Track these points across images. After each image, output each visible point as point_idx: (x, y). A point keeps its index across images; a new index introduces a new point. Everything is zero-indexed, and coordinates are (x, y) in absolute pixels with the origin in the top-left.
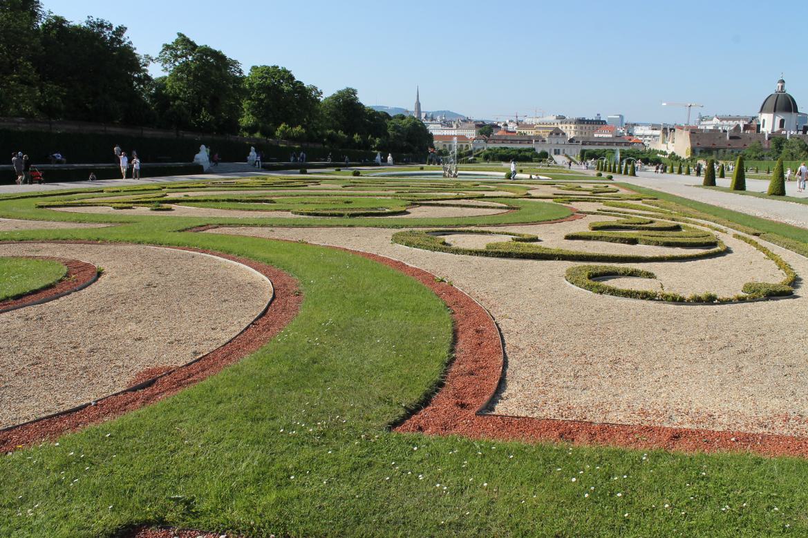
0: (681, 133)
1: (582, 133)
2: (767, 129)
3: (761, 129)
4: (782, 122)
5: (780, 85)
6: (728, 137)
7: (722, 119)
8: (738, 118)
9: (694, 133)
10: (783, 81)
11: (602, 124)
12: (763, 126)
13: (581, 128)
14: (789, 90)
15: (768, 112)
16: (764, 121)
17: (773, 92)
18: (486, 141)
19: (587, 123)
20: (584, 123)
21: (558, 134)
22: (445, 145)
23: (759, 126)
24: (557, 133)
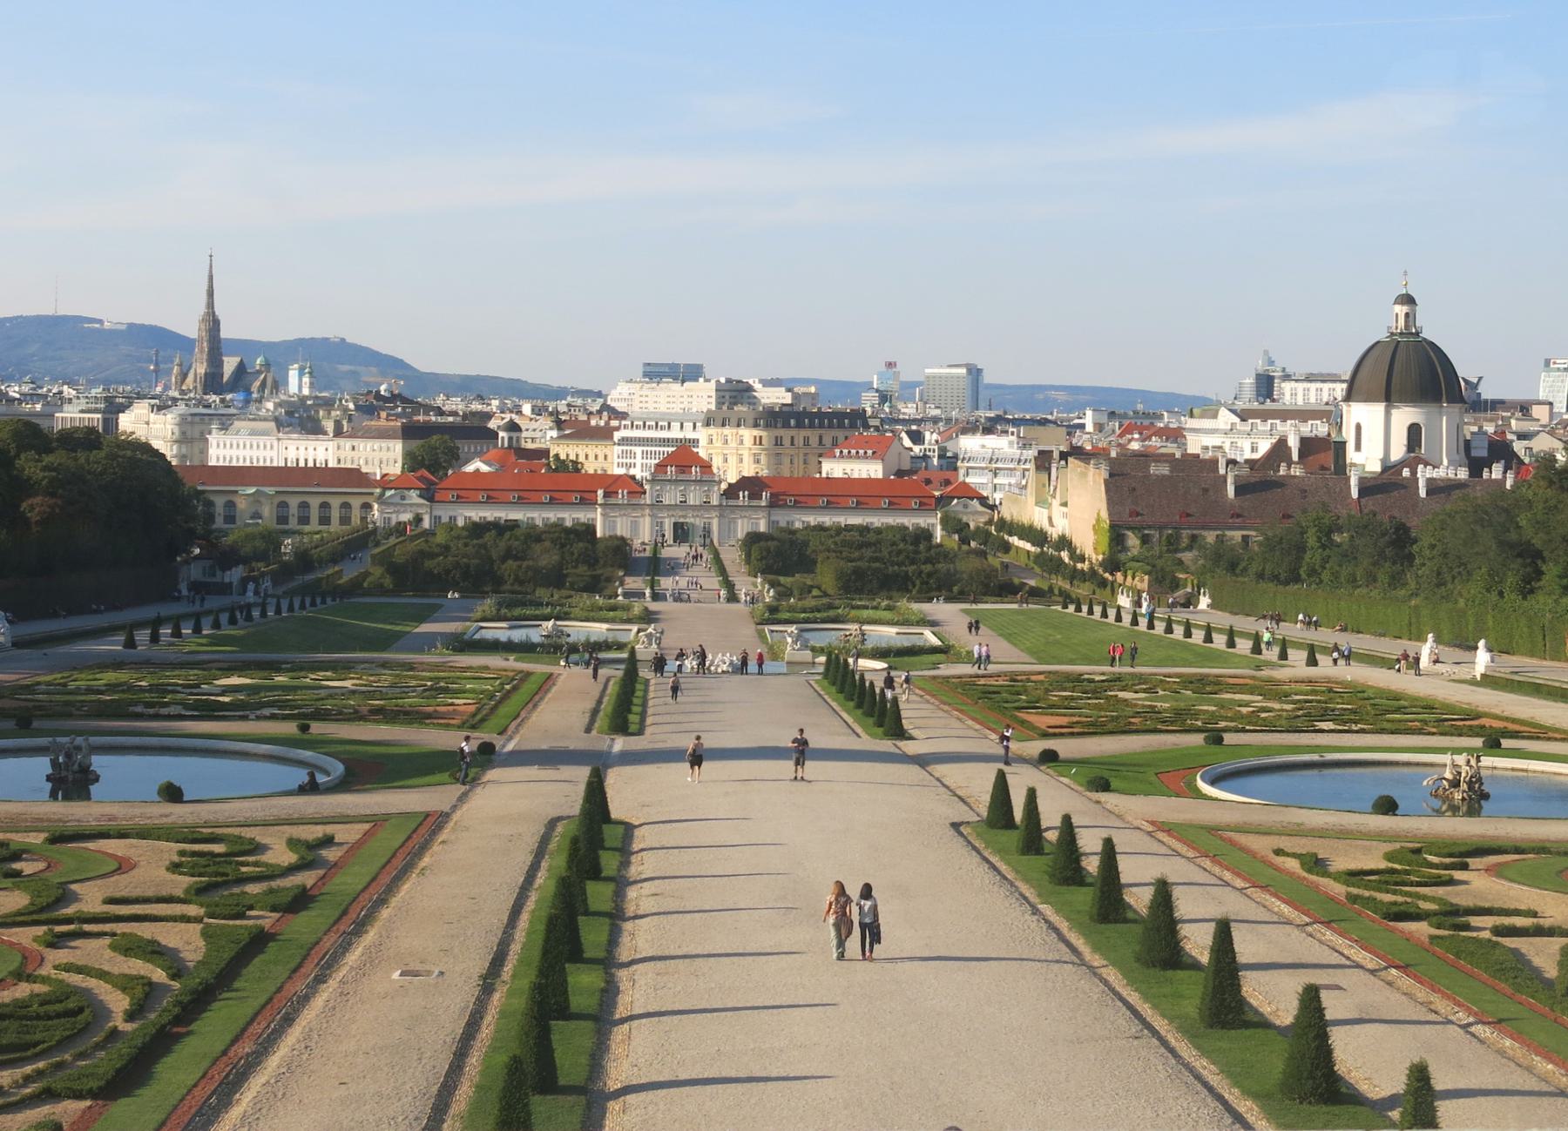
0: (1084, 475)
2: (1366, 459)
3: (1352, 456)
4: (1414, 432)
6: (1231, 490)
10: (1408, 300)
11: (853, 426)
12: (1358, 447)
15: (1369, 398)
16: (1358, 427)
19: (799, 425)
20: (786, 425)
21: (683, 468)
22: (283, 505)
23: (1342, 445)
24: (683, 461)
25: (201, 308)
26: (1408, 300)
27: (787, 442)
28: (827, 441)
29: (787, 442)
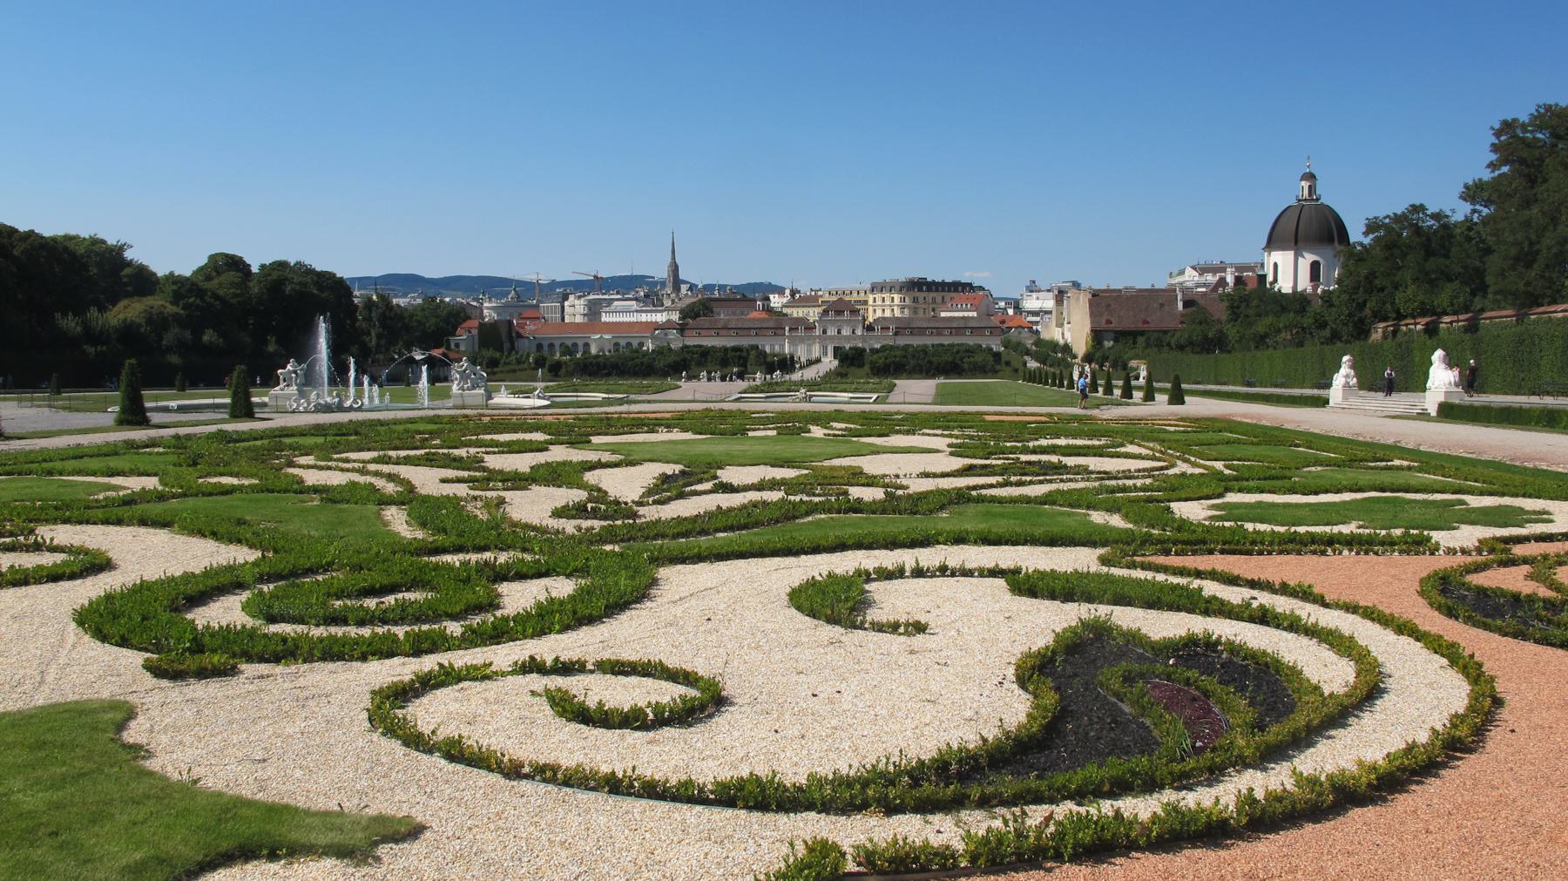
1: (915, 311)
4: (1315, 267)
5: (1305, 184)
6: (1180, 305)
7: (1202, 270)
8: (1221, 268)
9: (1101, 301)
10: (1310, 177)
13: (915, 300)
14: (1329, 196)
16: (1276, 265)
17: (1293, 202)
18: (682, 329)
19: (929, 290)
20: (920, 290)
21: (839, 312)
25: (669, 260)
26: (1310, 177)
27: (921, 300)
28: (947, 299)
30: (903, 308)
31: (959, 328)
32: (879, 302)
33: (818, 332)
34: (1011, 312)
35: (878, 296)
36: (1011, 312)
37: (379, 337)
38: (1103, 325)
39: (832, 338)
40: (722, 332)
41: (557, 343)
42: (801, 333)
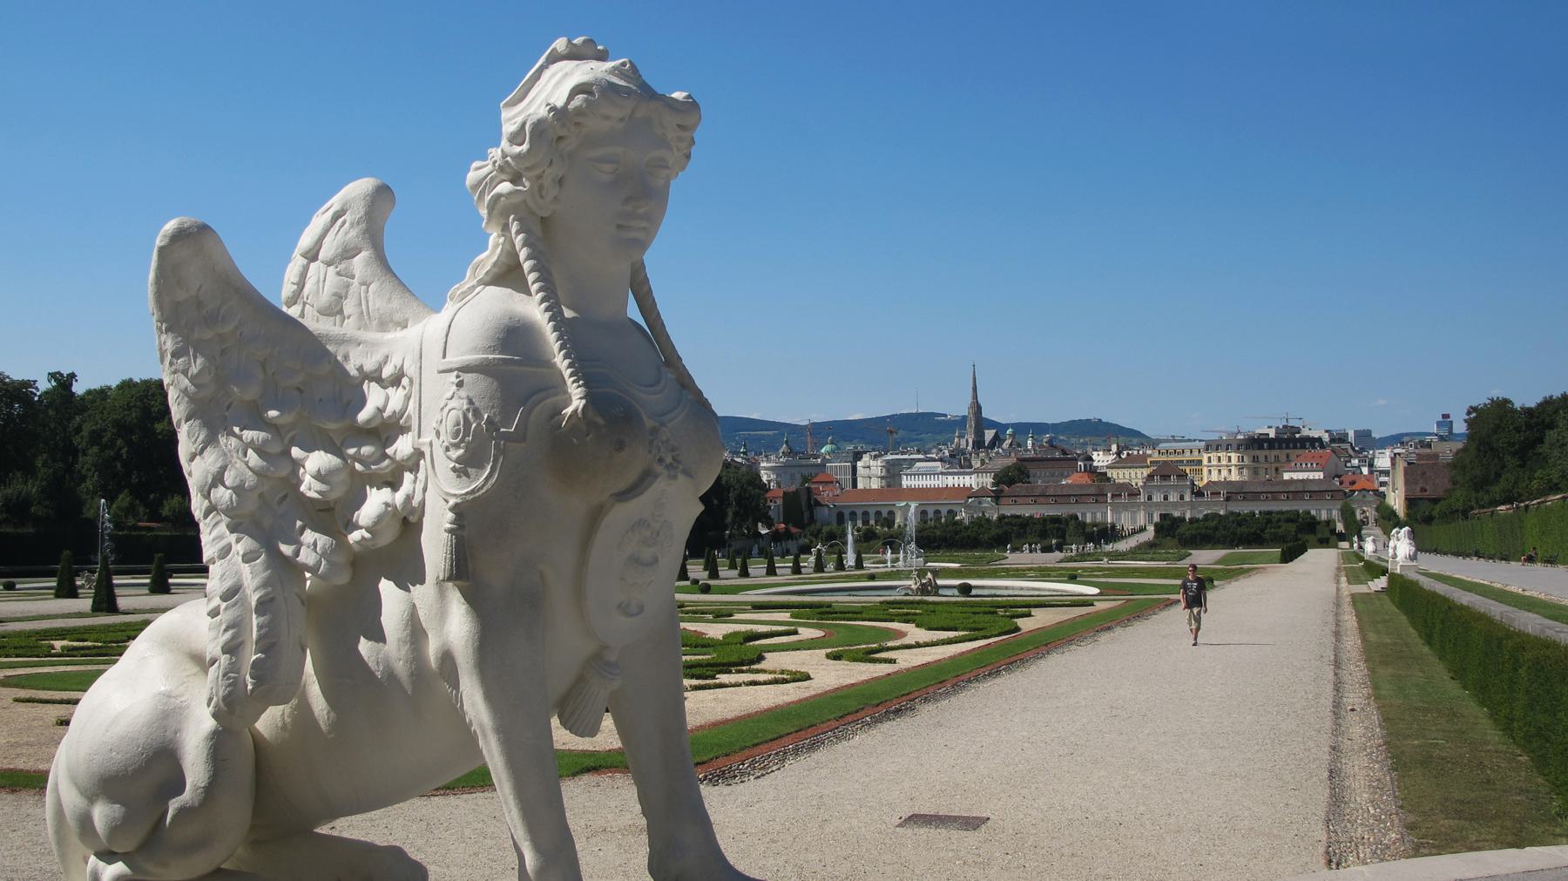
1: (1255, 472)
13: (1255, 459)
18: (997, 497)
19: (1271, 447)
20: (1261, 448)
21: (1165, 477)
25: (970, 400)
27: (1262, 459)
28: (1293, 457)
29: (1262, 459)
30: (1241, 468)
31: (1299, 491)
32: (1214, 462)
33: (1142, 498)
34: (1365, 470)
35: (1214, 455)
36: (1365, 470)
37: (735, 514)
38: (1418, 494)
39: (1158, 505)
40: (1042, 500)
41: (872, 512)
42: (1124, 500)
